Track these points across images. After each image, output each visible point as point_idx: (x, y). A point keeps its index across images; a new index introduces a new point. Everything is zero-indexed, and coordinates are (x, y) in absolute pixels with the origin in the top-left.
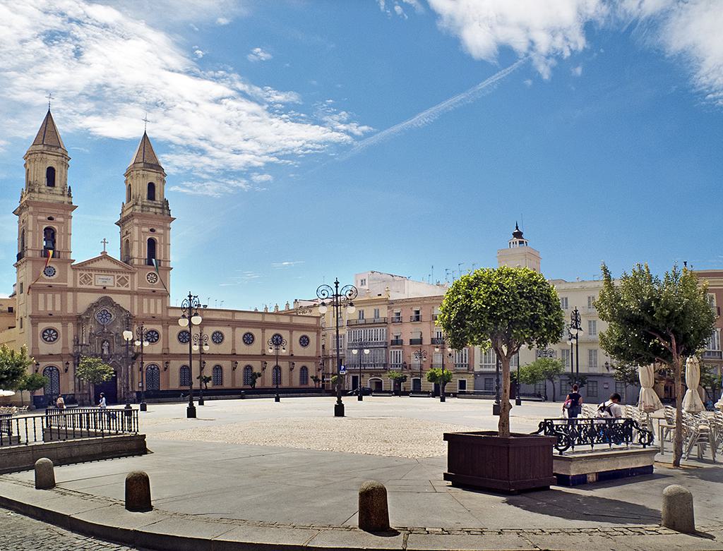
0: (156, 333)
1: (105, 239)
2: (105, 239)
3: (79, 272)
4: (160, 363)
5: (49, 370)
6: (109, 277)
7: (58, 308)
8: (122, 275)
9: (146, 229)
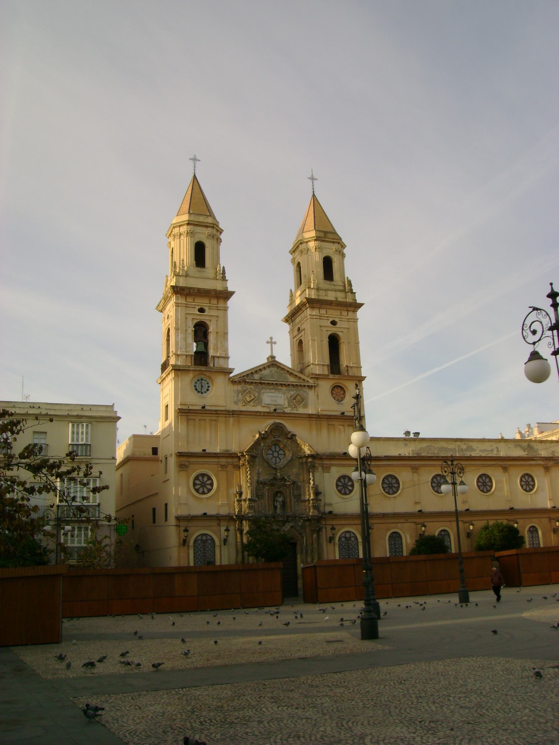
1: (271, 338)
2: (271, 338)
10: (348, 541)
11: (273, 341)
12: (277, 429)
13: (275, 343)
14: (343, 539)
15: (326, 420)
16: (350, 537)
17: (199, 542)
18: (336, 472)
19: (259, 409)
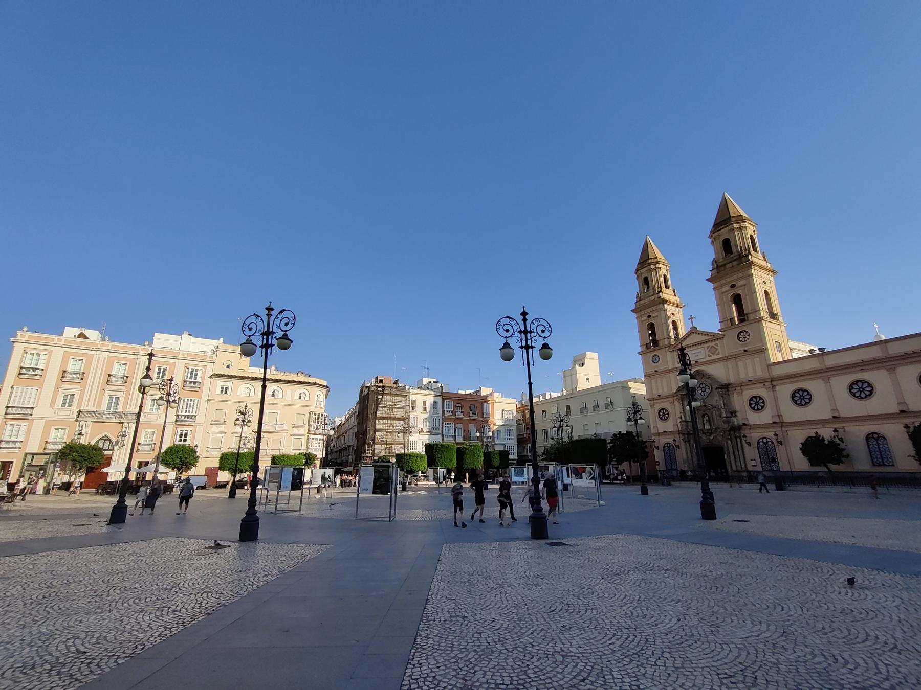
0: (761, 398)
2: (691, 316)
4: (770, 434)
6: (699, 350)
7: (666, 390)
8: (711, 344)
9: (727, 288)
14: (761, 443)
16: (767, 442)
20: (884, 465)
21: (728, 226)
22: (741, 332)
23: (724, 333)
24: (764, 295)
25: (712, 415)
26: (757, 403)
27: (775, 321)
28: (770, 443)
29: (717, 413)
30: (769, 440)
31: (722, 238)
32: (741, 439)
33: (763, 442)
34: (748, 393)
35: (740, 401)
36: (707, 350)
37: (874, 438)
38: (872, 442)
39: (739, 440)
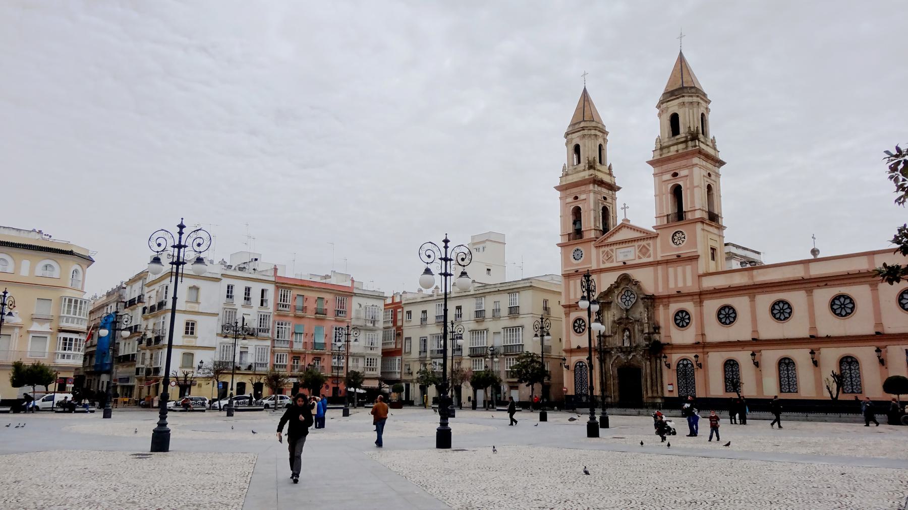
0: (687, 314)
1: (625, 204)
2: (625, 204)
3: (602, 250)
4: (691, 356)
5: (579, 366)
6: (629, 249)
9: (668, 176)
10: (685, 367)
11: (623, 207)
12: (625, 279)
13: (628, 208)
14: (681, 366)
15: (666, 264)
16: (687, 364)
17: (578, 367)
18: (674, 307)
19: (614, 264)
20: (790, 392)
21: (678, 98)
22: (676, 232)
23: (659, 231)
24: (706, 190)
25: (634, 330)
26: (682, 319)
27: (713, 224)
28: (690, 366)
29: (640, 328)
30: (689, 362)
31: (671, 112)
32: (661, 360)
33: (683, 364)
34: (674, 307)
35: (665, 315)
36: (637, 251)
37: (785, 363)
38: (784, 367)
39: (658, 361)
